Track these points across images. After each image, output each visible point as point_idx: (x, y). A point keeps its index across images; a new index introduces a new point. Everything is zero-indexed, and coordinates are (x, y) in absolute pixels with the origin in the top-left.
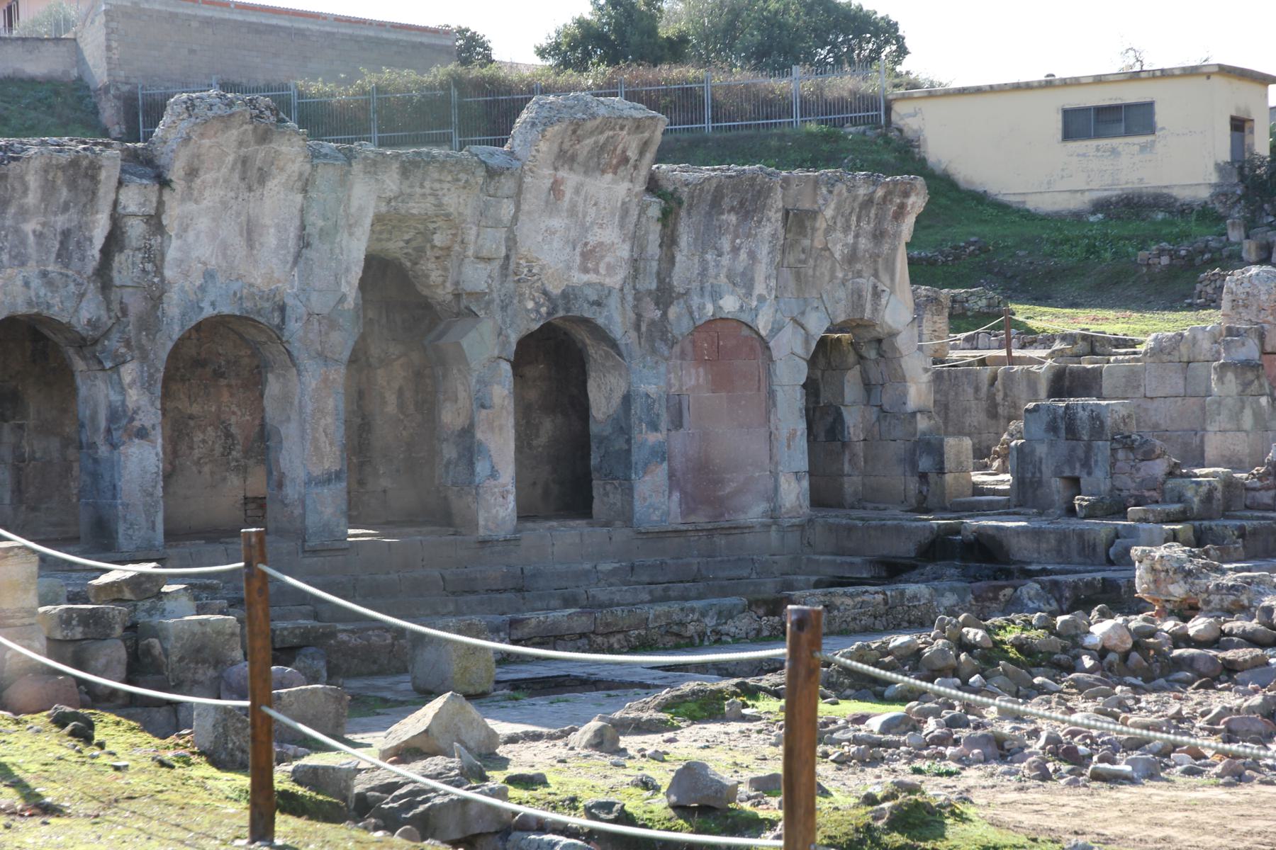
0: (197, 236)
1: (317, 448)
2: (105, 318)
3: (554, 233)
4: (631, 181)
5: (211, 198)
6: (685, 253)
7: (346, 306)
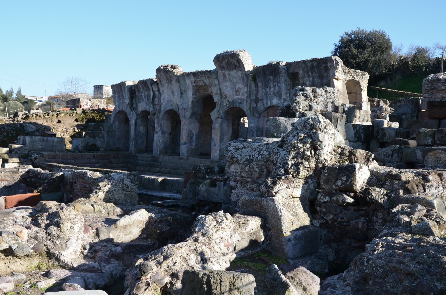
1: (183, 137)
4: (241, 71)
5: (166, 85)
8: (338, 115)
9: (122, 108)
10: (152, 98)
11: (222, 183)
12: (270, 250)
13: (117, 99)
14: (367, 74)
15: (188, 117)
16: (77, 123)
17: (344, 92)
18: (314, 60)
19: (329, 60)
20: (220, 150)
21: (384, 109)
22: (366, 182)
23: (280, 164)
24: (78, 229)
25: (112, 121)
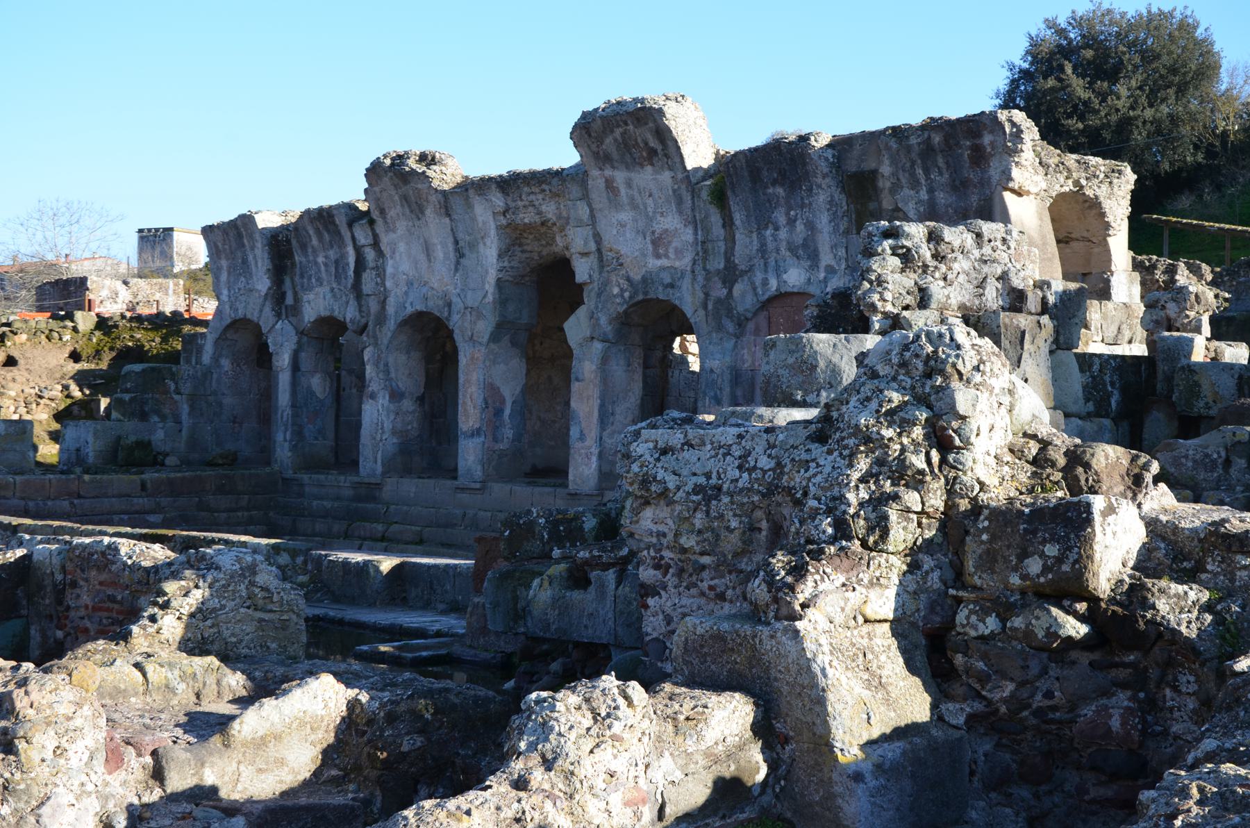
0: (400, 255)
1: (465, 410)
2: (358, 317)
3: (625, 226)
4: (670, 169)
5: (402, 226)
6: (742, 231)
7: (487, 300)
8: (1023, 321)
9: (245, 307)
10: (351, 273)
11: (611, 575)
12: (789, 815)
13: (224, 277)
14: (1128, 170)
15: (487, 337)
16: (78, 366)
17: (1043, 237)
18: (934, 125)
19: (987, 122)
20: (601, 456)
21: (1193, 297)
22: (1131, 564)
23: (819, 500)
24: (86, 757)
25: (206, 358)
